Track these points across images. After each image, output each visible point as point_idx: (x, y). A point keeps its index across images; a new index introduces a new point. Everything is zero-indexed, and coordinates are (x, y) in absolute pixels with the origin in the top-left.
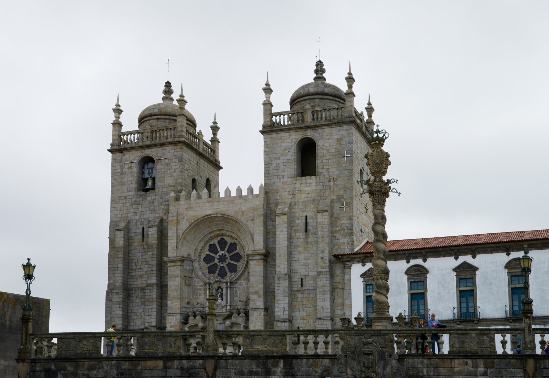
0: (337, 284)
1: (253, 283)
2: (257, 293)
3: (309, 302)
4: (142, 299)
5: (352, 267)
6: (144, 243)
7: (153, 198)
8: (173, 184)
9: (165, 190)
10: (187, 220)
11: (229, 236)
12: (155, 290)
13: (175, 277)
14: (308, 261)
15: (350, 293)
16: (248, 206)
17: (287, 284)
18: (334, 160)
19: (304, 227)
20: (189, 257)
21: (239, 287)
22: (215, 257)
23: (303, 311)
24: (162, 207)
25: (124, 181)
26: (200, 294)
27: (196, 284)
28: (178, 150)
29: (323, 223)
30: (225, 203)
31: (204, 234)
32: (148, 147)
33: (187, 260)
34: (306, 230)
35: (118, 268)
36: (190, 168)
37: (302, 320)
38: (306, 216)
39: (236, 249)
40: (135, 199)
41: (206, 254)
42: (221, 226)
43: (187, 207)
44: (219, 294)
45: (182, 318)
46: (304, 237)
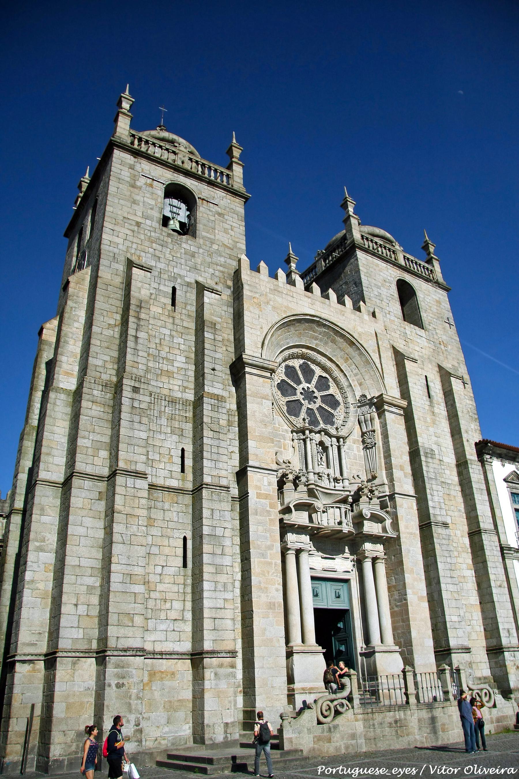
1: (394, 451)
2: (402, 468)
4: (173, 422)
5: (492, 464)
6: (177, 315)
7: (193, 249)
8: (231, 246)
9: (215, 247)
10: (274, 308)
11: (318, 364)
13: (263, 398)
18: (438, 321)
21: (348, 453)
24: (211, 271)
25: (137, 198)
26: (284, 446)
27: (277, 426)
28: (236, 204)
29: (459, 392)
31: (288, 343)
32: (187, 174)
35: (136, 337)
38: (426, 376)
39: (328, 388)
40: (157, 235)
41: (281, 378)
43: (272, 288)
46: (428, 403)
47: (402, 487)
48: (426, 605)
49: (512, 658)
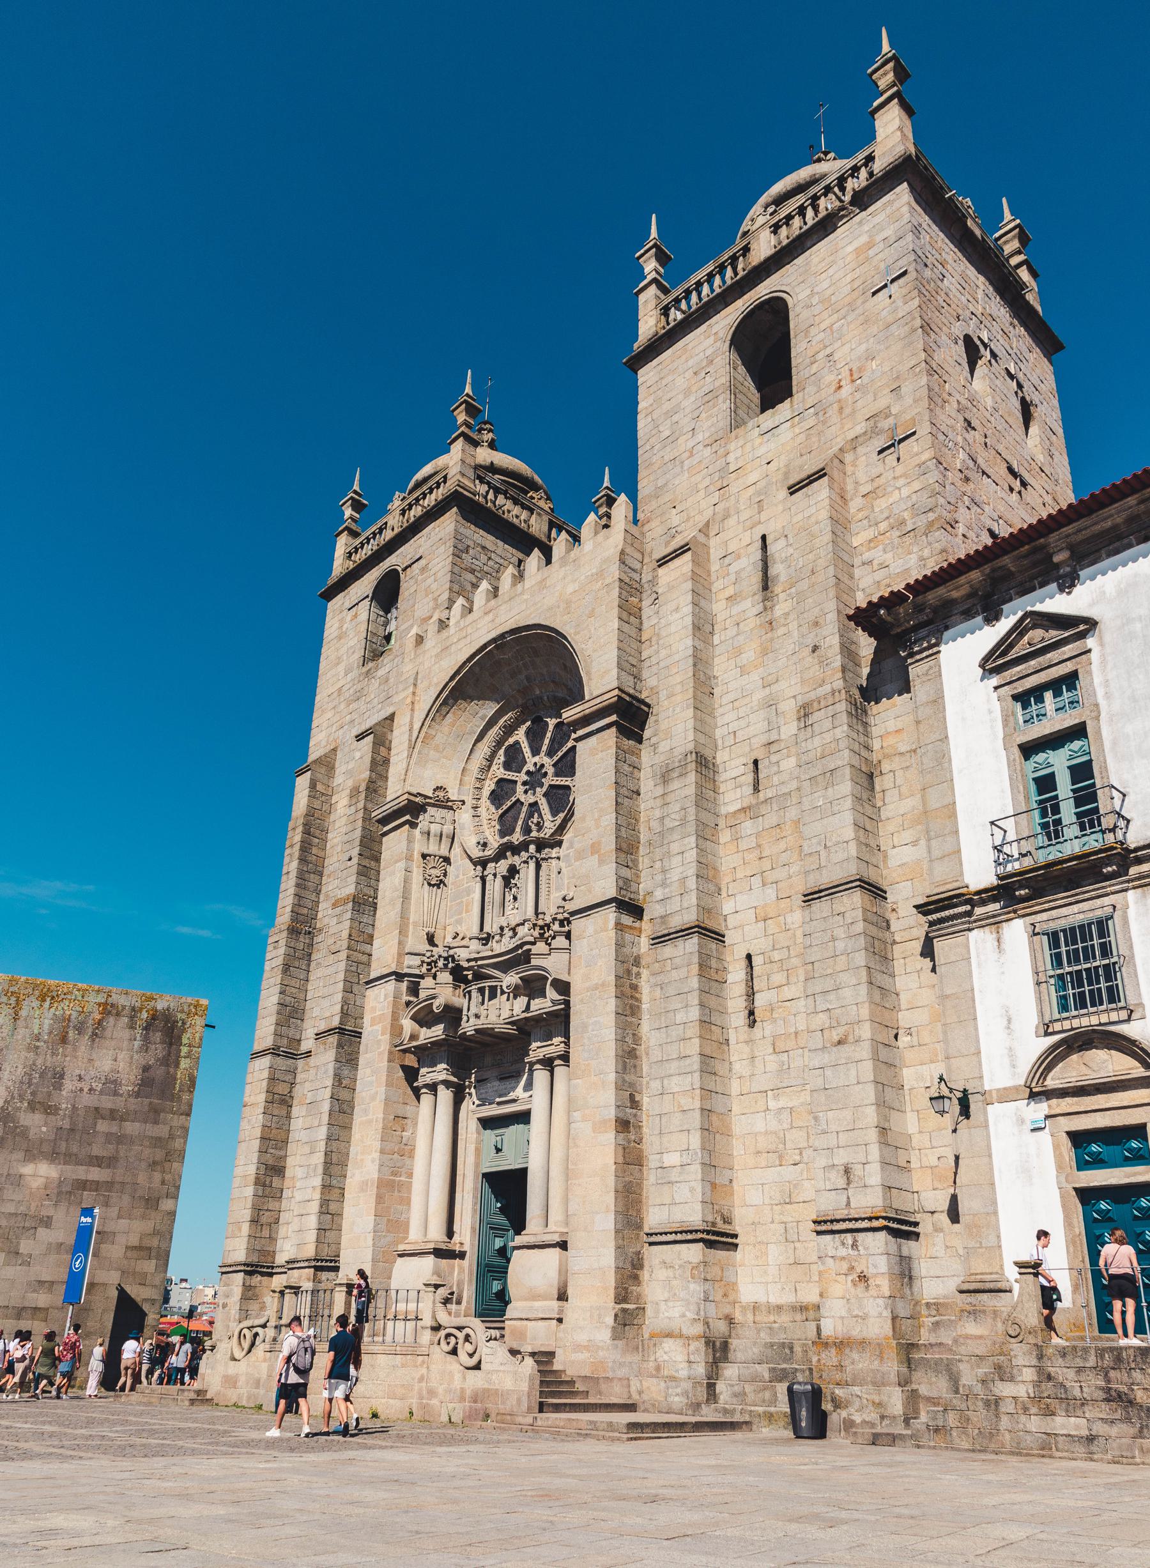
0: (891, 741)
1: (583, 819)
2: (595, 848)
3: (782, 845)
12: (349, 915)
14: (775, 688)
15: (943, 758)
16: (583, 577)
17: (691, 790)
19: (757, 578)
20: (441, 794)
22: (516, 782)
23: (764, 885)
30: (525, 597)
33: (434, 805)
34: (766, 584)
36: (486, 568)
37: (761, 924)
42: (522, 677)
44: (514, 890)
45: (404, 986)
47: (590, 892)
48: (609, 1138)
49: (842, 1252)
